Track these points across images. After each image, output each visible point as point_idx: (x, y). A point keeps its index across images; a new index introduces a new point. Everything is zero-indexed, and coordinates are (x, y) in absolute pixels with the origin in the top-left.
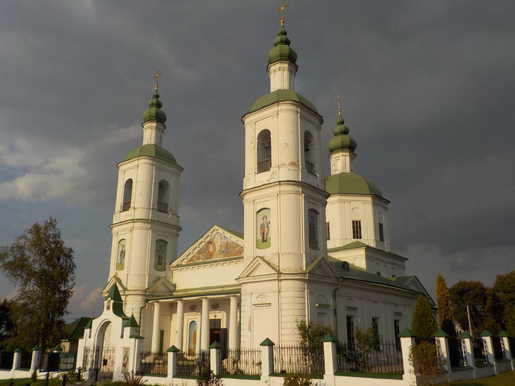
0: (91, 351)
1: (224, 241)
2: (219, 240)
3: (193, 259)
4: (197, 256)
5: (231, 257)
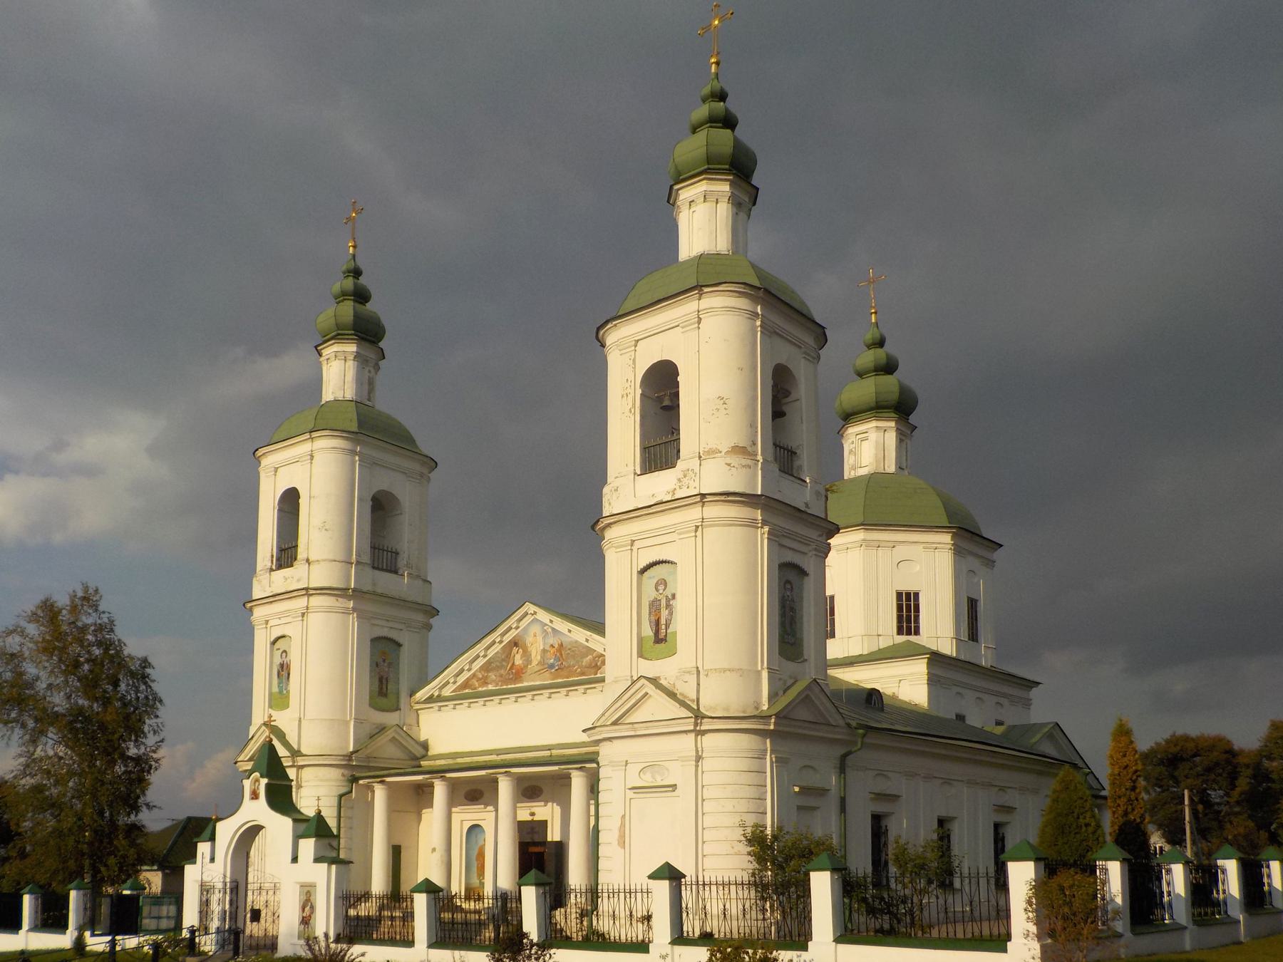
0: (217, 891)
1: (552, 640)
2: (540, 639)
3: (470, 683)
4: (481, 676)
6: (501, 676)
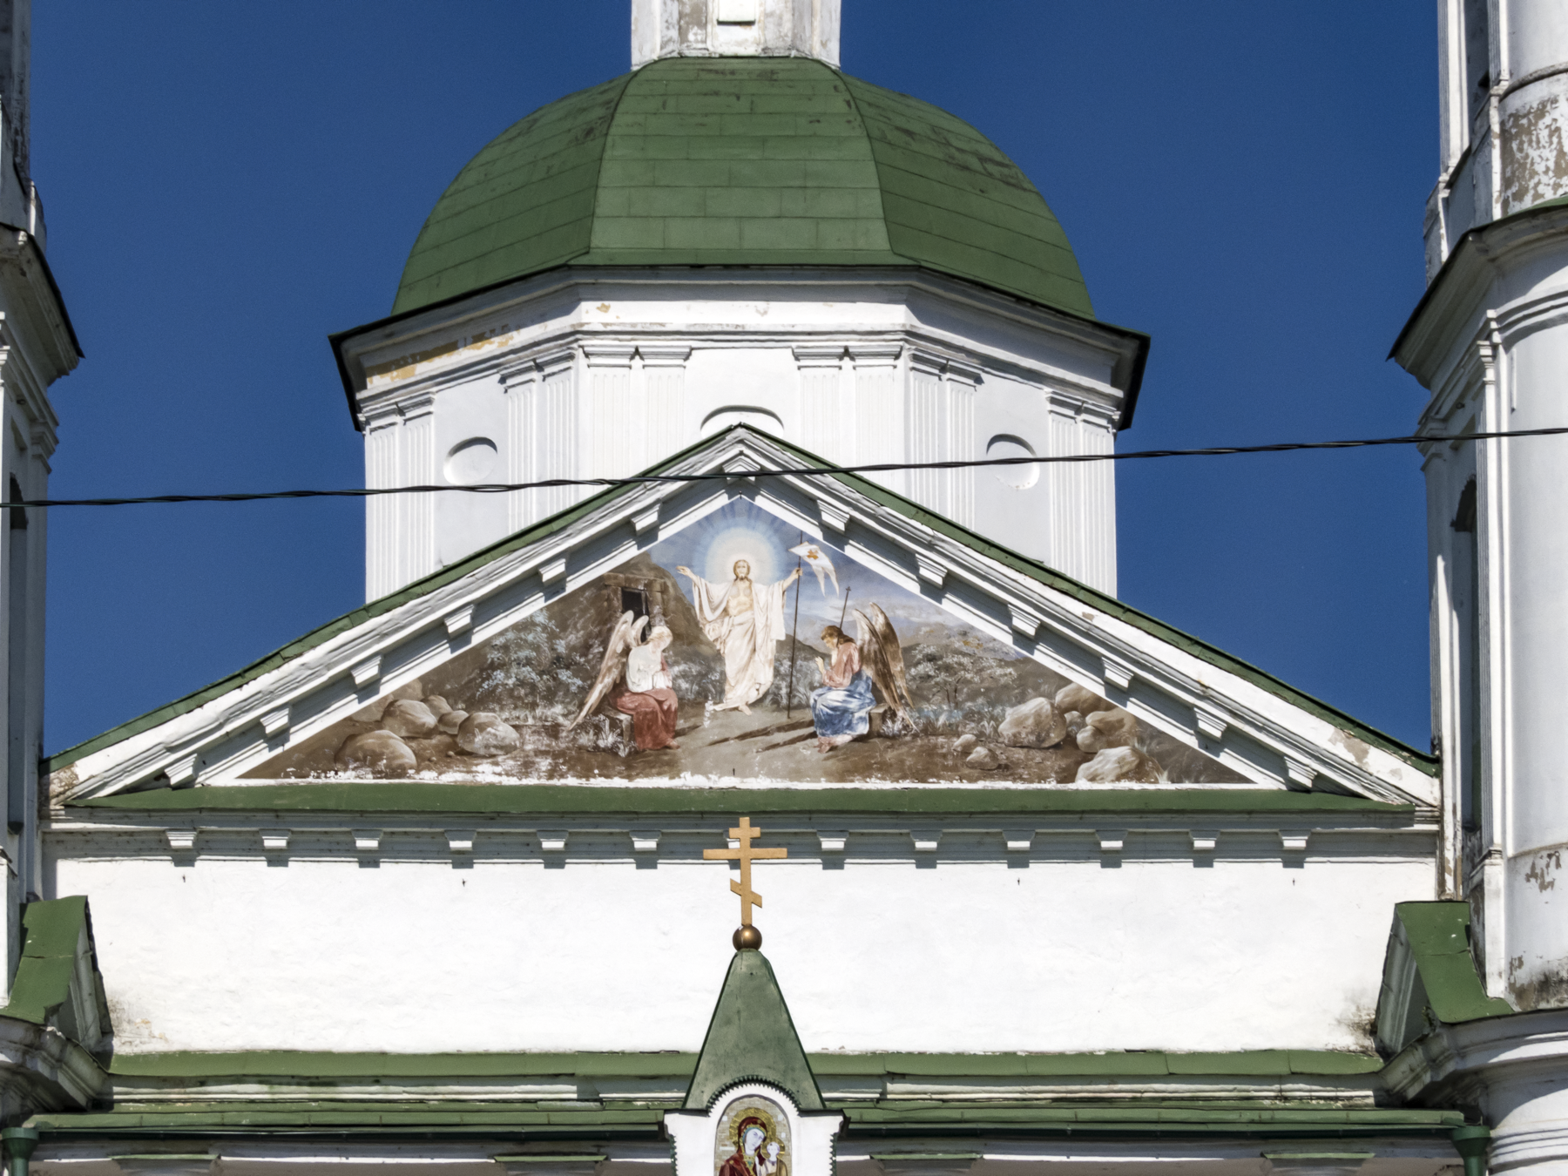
3: (369, 741)
4: (430, 720)
5: (944, 785)
6: (553, 730)
